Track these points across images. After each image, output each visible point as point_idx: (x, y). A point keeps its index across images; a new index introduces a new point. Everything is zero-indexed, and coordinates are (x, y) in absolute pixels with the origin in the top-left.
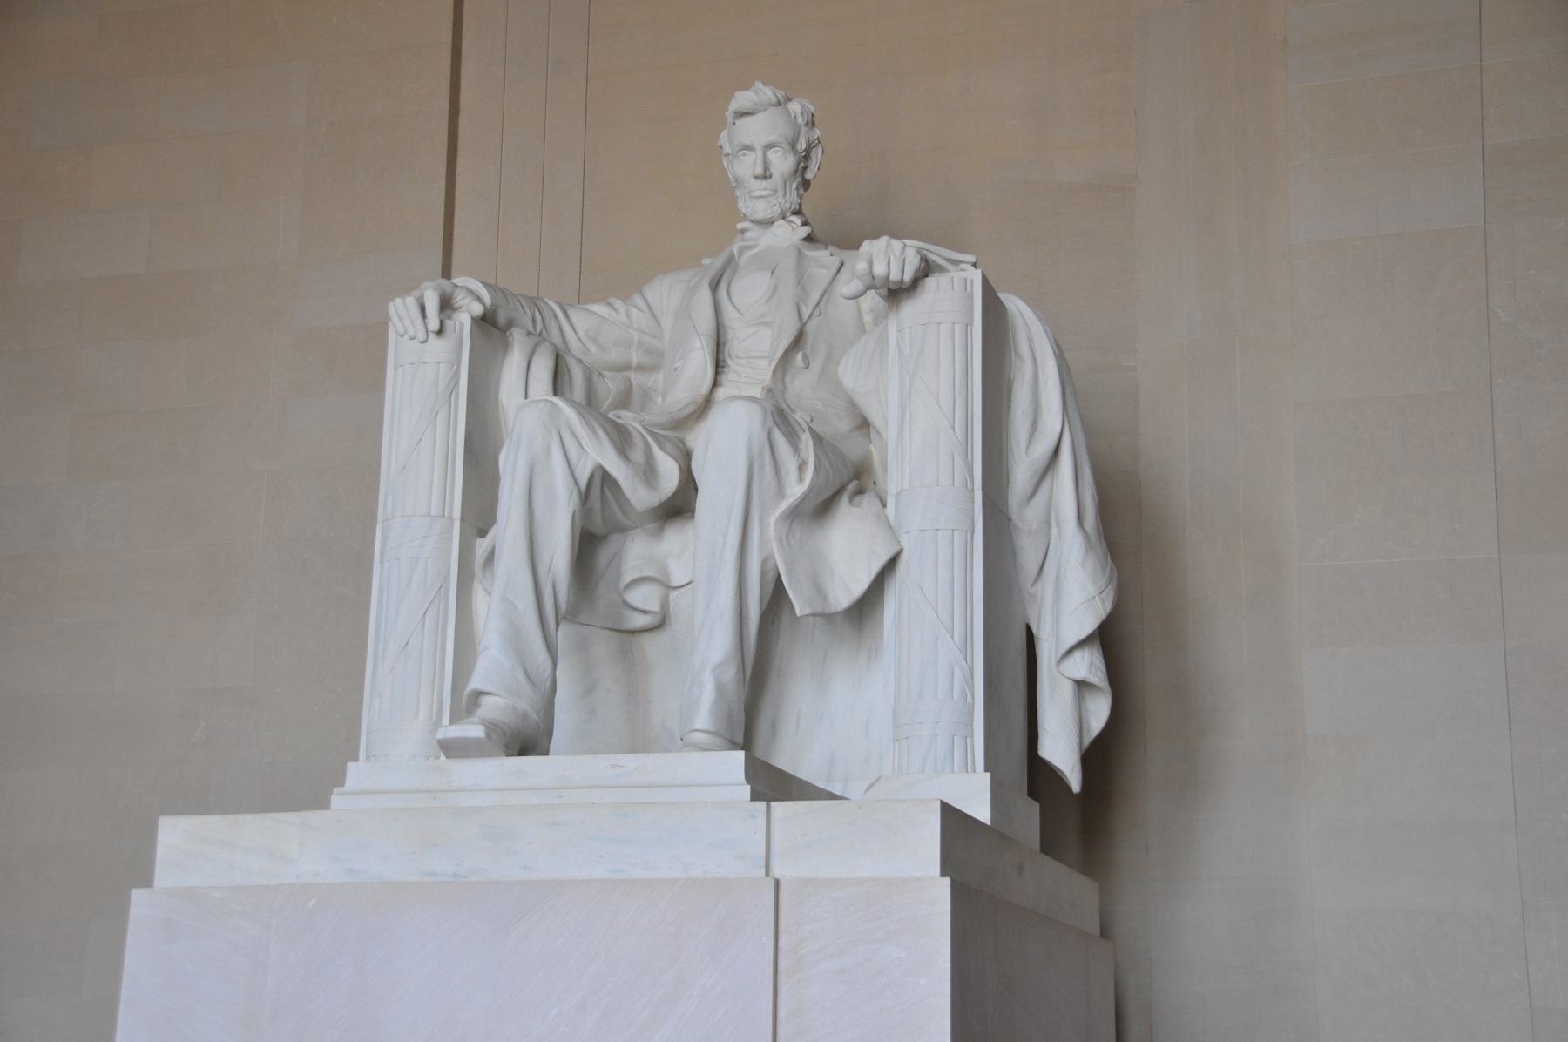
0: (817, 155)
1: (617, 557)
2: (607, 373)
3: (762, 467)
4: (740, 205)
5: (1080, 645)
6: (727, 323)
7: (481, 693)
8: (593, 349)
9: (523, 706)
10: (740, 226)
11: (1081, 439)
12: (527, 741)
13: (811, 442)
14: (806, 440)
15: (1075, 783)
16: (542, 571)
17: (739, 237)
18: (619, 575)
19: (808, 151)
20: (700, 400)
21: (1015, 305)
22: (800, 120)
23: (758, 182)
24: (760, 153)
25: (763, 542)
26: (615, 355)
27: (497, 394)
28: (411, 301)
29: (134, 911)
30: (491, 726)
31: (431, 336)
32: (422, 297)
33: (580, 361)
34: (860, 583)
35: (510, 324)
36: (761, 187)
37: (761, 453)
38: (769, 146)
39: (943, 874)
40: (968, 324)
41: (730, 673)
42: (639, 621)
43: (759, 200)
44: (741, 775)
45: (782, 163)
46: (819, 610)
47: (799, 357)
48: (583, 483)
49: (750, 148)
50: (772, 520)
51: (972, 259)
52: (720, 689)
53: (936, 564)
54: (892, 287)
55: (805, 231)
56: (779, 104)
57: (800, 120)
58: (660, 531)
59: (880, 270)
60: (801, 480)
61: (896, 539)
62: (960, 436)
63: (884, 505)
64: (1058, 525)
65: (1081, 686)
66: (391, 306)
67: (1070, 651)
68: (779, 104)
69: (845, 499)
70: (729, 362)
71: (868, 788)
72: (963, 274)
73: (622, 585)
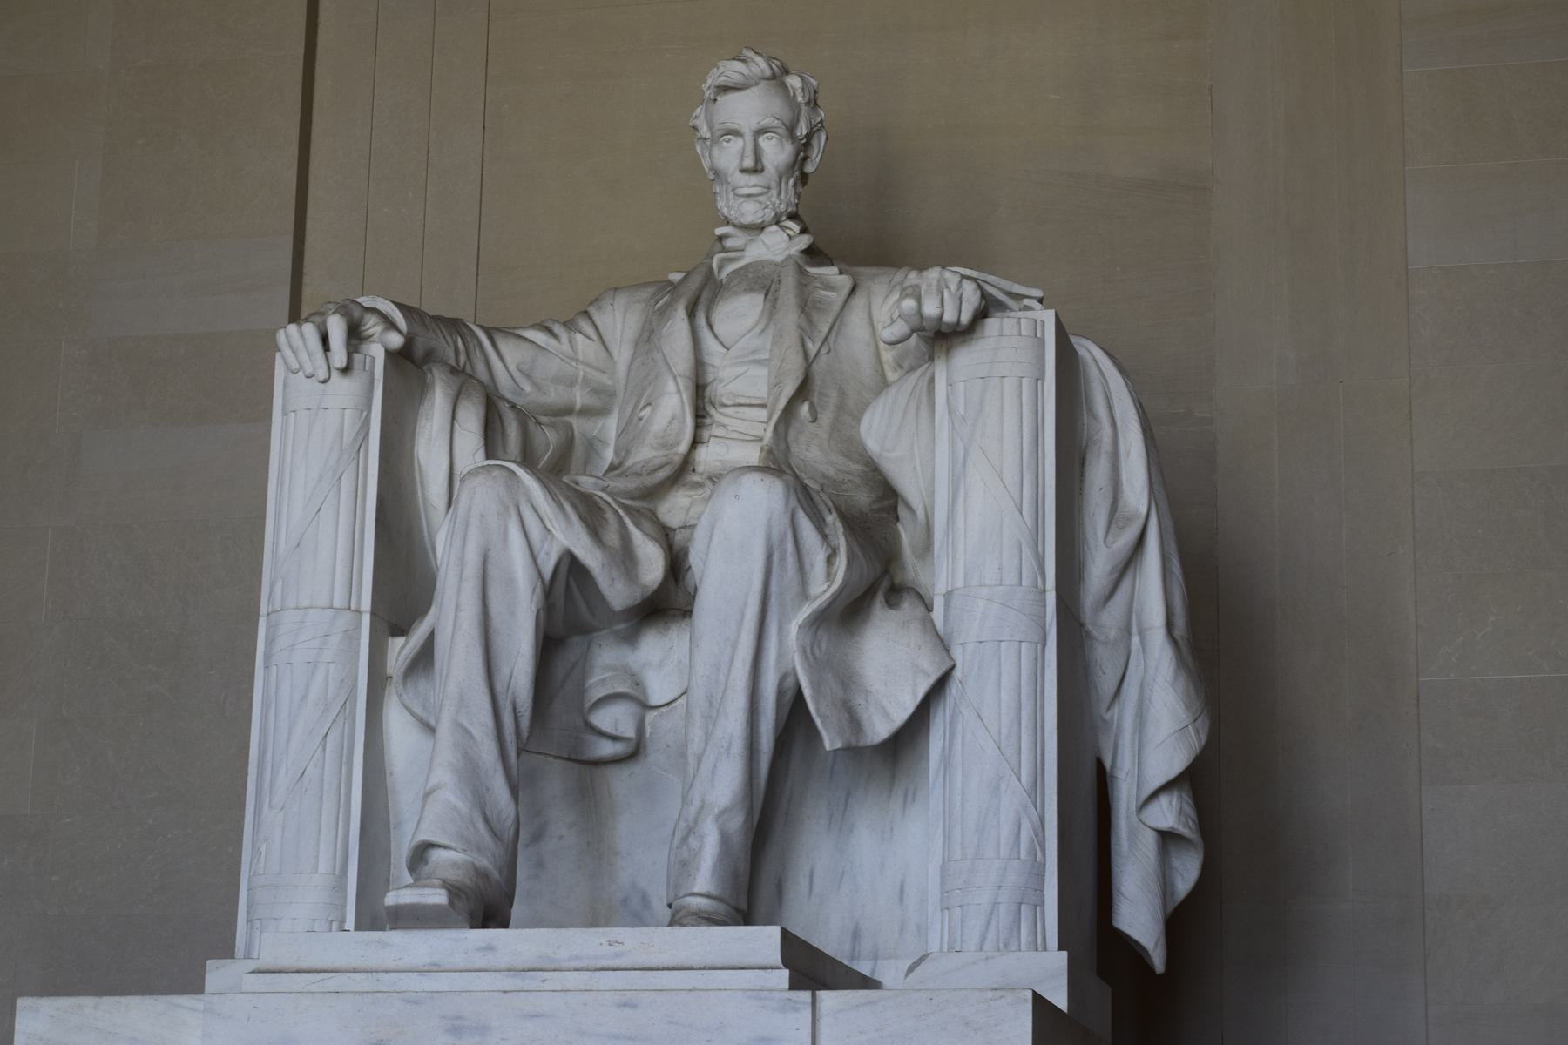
0: (820, 142)
1: (583, 668)
2: (543, 419)
3: (783, 559)
4: (721, 204)
6: (707, 359)
7: (431, 845)
8: (527, 388)
9: (484, 862)
11: (1169, 523)
12: (487, 906)
13: (839, 525)
14: (831, 518)
15: (1158, 961)
16: (500, 687)
18: (581, 691)
19: (809, 136)
20: (678, 459)
21: (1090, 352)
22: (800, 99)
23: (747, 177)
24: (749, 138)
25: (781, 655)
26: (554, 396)
27: (412, 447)
28: (309, 329)
30: (454, 891)
32: (324, 323)
33: (513, 406)
34: (902, 708)
35: (430, 356)
36: (749, 184)
37: (782, 541)
40: (1040, 377)
41: (736, 822)
42: (607, 749)
43: (747, 199)
44: (775, 956)
45: (776, 153)
46: (854, 743)
48: (548, 571)
49: (736, 133)
50: (793, 628)
51: (1039, 293)
52: (725, 839)
53: (999, 685)
54: (944, 329)
55: (804, 241)
56: (774, 77)
58: (631, 638)
59: (930, 309)
60: (829, 576)
61: (947, 650)
62: (1029, 522)
63: (929, 609)
64: (1141, 633)
65: (1166, 838)
66: (281, 335)
67: (1155, 795)
69: (880, 598)
70: (712, 411)
71: (911, 970)
72: (1028, 314)
73: (587, 705)
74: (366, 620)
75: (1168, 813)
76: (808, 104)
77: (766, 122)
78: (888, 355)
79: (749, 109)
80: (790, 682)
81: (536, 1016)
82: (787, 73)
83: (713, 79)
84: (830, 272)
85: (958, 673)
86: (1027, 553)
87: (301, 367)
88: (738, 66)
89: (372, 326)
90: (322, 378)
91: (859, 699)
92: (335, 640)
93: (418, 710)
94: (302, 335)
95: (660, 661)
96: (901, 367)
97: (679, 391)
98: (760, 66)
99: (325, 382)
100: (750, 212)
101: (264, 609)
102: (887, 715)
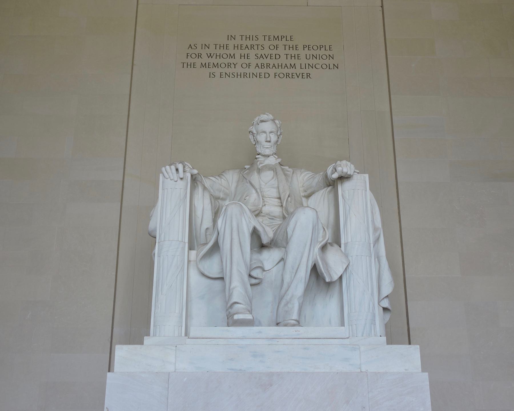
9: (249, 308)
10: (257, 156)
23: (267, 143)
26: (217, 194)
28: (173, 167)
29: (108, 381)
36: (267, 145)
38: (271, 132)
39: (423, 371)
42: (254, 281)
45: (274, 138)
47: (289, 199)
49: (265, 132)
51: (358, 171)
55: (279, 160)
59: (345, 170)
63: (340, 247)
65: (385, 309)
66: (163, 169)
74: (187, 245)
75: (386, 304)
78: (302, 189)
79: (268, 127)
81: (278, 352)
84: (287, 168)
85: (351, 264)
87: (169, 177)
88: (265, 115)
89: (187, 169)
90: (176, 180)
91: (329, 269)
93: (202, 270)
94: (171, 168)
95: (269, 258)
96: (305, 191)
97: (257, 192)
98: (271, 117)
100: (267, 152)
102: (336, 273)
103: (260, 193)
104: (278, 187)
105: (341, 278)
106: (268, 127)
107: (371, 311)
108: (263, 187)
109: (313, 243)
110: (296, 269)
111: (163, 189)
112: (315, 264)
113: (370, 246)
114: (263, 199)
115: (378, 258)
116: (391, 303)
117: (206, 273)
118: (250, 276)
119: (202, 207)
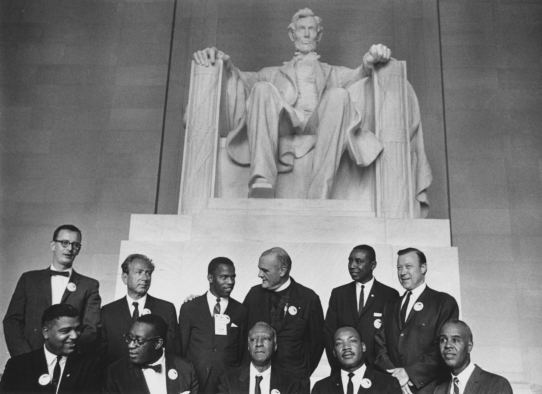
0: (321, 34)
3: (347, 111)
5: (425, 191)
7: (259, 177)
10: (296, 53)
17: (294, 57)
24: (307, 29)
25: (344, 139)
31: (210, 65)
36: (306, 40)
41: (330, 184)
42: (284, 168)
45: (313, 34)
49: (303, 28)
55: (319, 56)
57: (318, 22)
63: (375, 133)
64: (416, 151)
66: (195, 55)
67: (420, 193)
68: (312, 16)
74: (217, 131)
75: (423, 198)
76: (320, 24)
77: (313, 24)
80: (345, 147)
82: (315, 15)
83: (297, 14)
84: (326, 64)
85: (385, 150)
86: (402, 120)
87: (201, 62)
90: (207, 65)
92: (209, 134)
93: (231, 155)
94: (202, 54)
99: (208, 67)
101: (187, 126)
103: (295, 85)
104: (315, 82)
105: (374, 164)
106: (308, 22)
107: (405, 198)
108: (300, 81)
109: (343, 126)
110: (325, 151)
111: (195, 75)
112: (346, 148)
113: (405, 133)
114: (299, 93)
115: (415, 151)
116: (429, 197)
117: (236, 159)
118: (279, 162)
119: (235, 95)
